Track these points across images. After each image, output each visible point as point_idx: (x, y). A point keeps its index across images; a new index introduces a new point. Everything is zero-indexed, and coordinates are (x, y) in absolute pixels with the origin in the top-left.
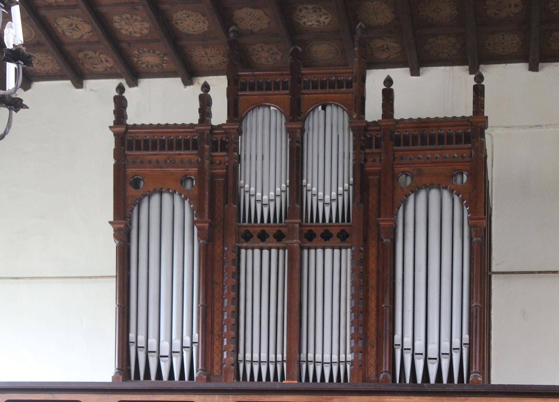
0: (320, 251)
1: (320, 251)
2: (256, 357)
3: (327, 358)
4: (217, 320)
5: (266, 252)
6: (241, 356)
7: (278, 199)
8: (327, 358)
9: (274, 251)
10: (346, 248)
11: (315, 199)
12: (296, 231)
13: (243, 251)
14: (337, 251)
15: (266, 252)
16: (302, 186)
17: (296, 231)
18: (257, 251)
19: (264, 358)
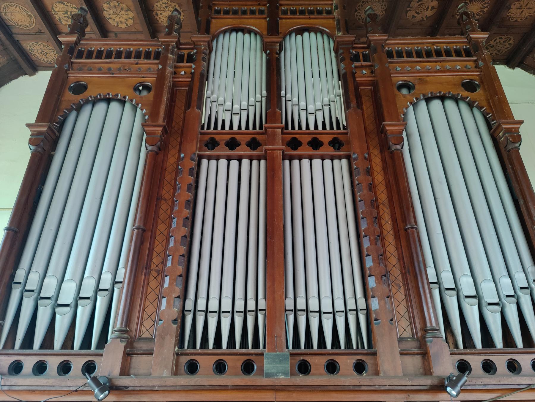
2: (213, 305)
3: (327, 306)
4: (158, 248)
6: (189, 305)
7: (251, 109)
8: (327, 306)
9: (245, 162)
10: (340, 158)
11: (296, 109)
12: (274, 140)
13: (205, 162)
14: (327, 162)
16: (280, 97)
17: (274, 140)
18: (223, 162)
19: (226, 306)
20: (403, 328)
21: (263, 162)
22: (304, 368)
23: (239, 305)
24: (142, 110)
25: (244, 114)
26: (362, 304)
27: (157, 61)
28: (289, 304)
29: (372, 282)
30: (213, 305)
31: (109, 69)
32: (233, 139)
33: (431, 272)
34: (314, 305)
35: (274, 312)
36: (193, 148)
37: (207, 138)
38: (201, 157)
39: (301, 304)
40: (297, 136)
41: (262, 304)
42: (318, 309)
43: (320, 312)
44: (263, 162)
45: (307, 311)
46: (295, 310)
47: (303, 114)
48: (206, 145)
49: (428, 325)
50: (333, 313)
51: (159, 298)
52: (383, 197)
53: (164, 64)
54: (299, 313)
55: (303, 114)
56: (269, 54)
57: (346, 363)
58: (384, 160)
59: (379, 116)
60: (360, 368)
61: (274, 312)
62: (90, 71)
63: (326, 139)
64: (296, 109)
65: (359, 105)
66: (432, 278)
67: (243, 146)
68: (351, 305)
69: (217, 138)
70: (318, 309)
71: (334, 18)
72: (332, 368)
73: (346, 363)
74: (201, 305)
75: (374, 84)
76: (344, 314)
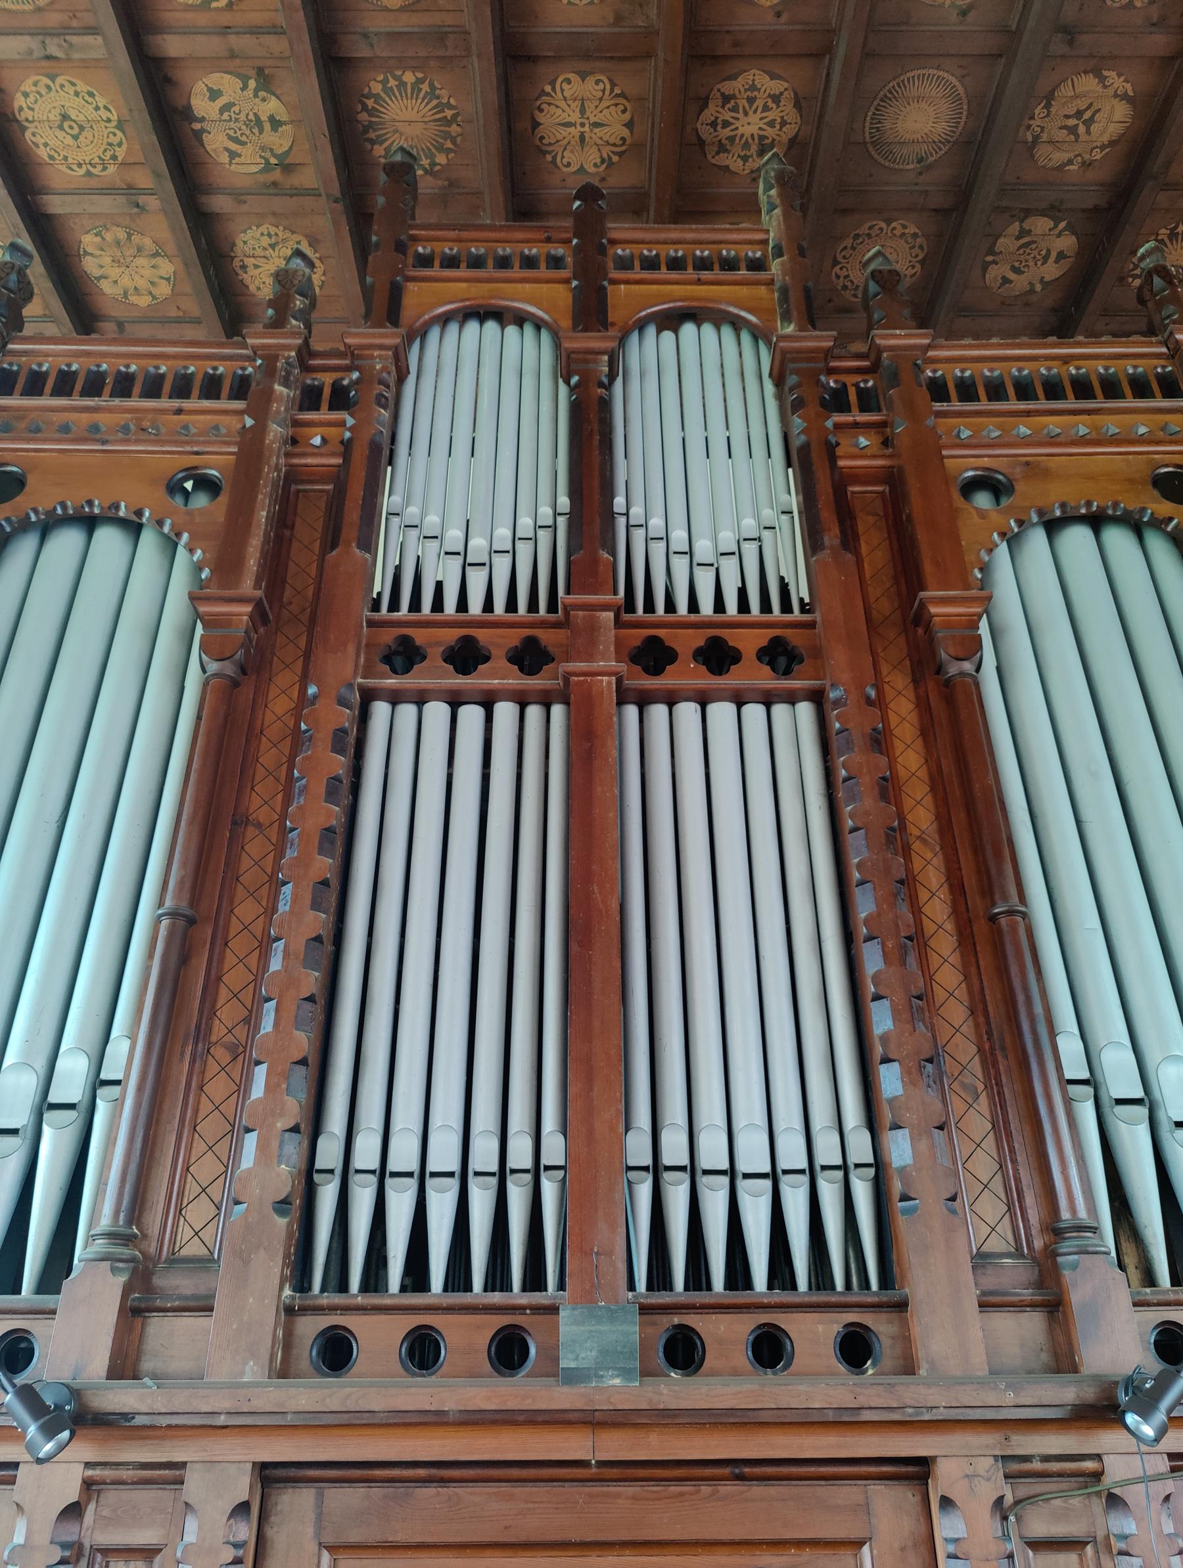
0: (688, 711)
1: (688, 711)
2: (404, 1155)
3: (754, 1157)
4: (235, 977)
5: (471, 715)
6: (329, 1153)
7: (524, 552)
8: (754, 1157)
9: (505, 711)
10: (791, 699)
11: (658, 549)
12: (592, 642)
13: (381, 709)
14: (754, 712)
15: (471, 715)
16: (609, 516)
17: (592, 642)
18: (437, 711)
19: (444, 1155)
20: (988, 1222)
21: (557, 711)
22: (684, 1352)
23: (484, 1154)
24: (192, 551)
25: (502, 566)
26: (860, 1147)
27: (239, 405)
28: (638, 1149)
29: (890, 1080)
30: (404, 1155)
31: (95, 428)
32: (468, 642)
33: (1070, 1047)
34: (713, 1153)
35: (591, 1171)
36: (344, 667)
37: (388, 637)
38: (368, 697)
39: (674, 1150)
40: (661, 633)
41: (554, 1149)
42: (725, 1165)
43: (731, 1172)
44: (557, 711)
45: (692, 1169)
46: (657, 1169)
47: (680, 566)
48: (387, 659)
49: (1065, 1215)
50: (774, 1176)
51: (237, 1131)
52: (922, 817)
53: (261, 412)
54: (667, 1176)
55: (680, 566)
56: (577, 386)
57: (814, 1336)
58: (923, 705)
59: (908, 575)
60: (855, 1349)
61: (591, 1171)
62: (35, 432)
63: (749, 642)
64: (658, 549)
65: (850, 540)
66: (1075, 1068)
67: (499, 662)
68: (827, 1152)
69: (419, 636)
70: (725, 1165)
71: (771, 282)
72: (770, 1349)
73: (814, 1336)
74: (366, 1153)
75: (893, 479)
76: (805, 1179)
